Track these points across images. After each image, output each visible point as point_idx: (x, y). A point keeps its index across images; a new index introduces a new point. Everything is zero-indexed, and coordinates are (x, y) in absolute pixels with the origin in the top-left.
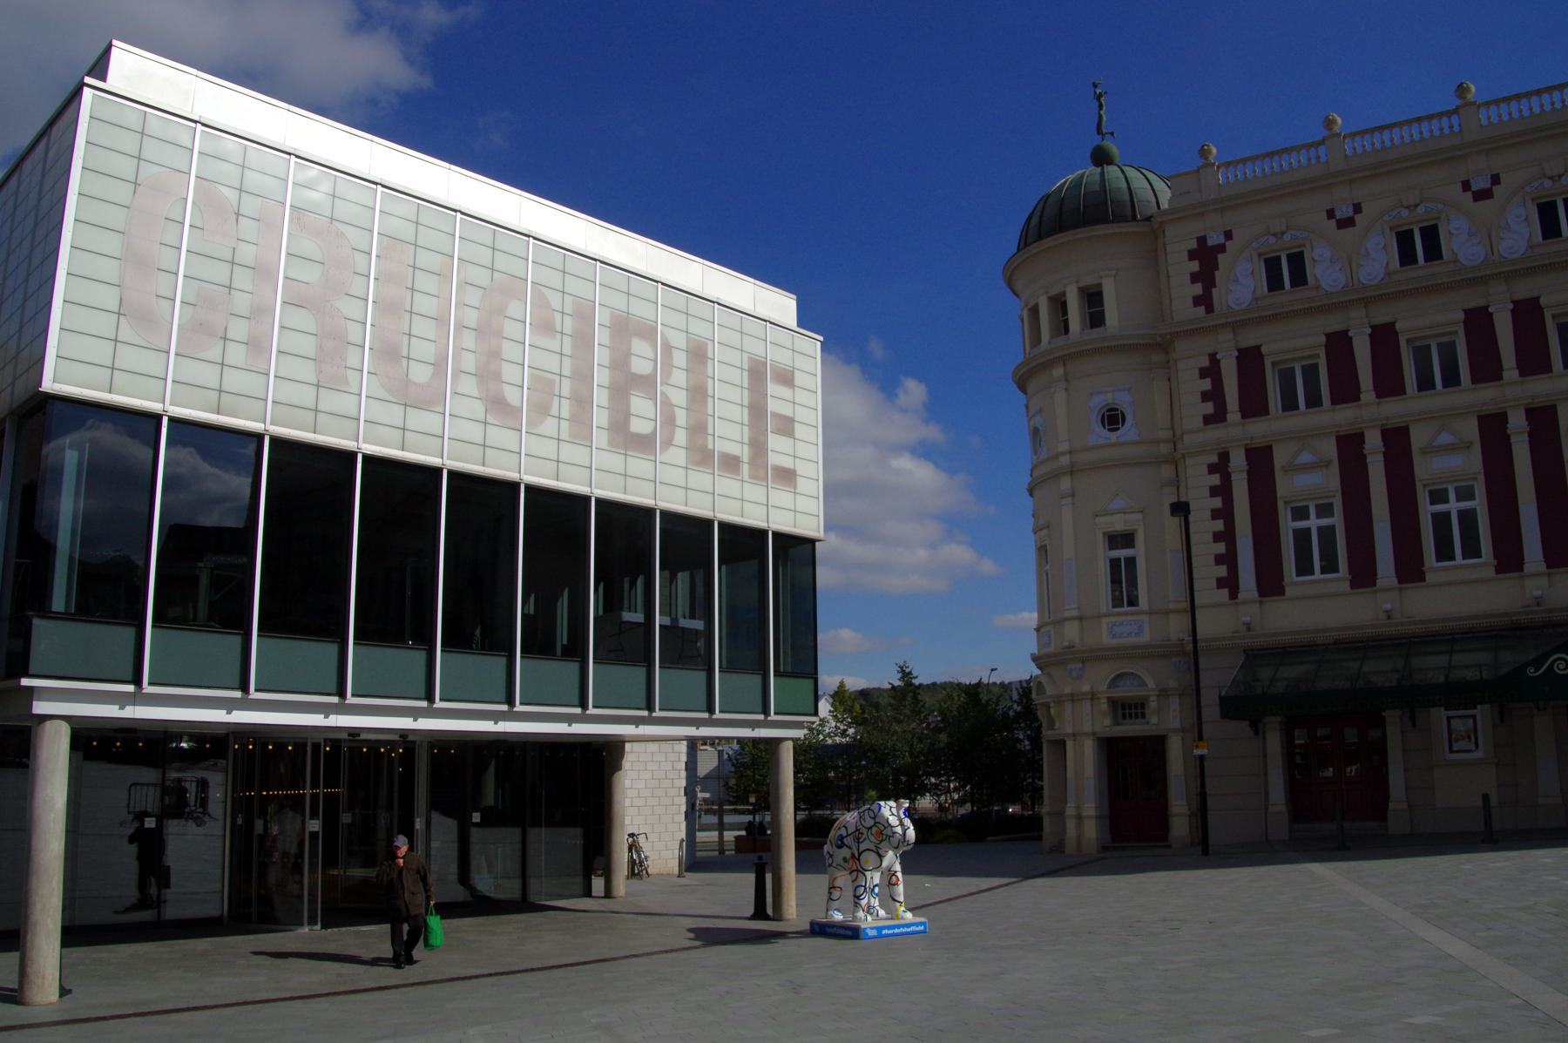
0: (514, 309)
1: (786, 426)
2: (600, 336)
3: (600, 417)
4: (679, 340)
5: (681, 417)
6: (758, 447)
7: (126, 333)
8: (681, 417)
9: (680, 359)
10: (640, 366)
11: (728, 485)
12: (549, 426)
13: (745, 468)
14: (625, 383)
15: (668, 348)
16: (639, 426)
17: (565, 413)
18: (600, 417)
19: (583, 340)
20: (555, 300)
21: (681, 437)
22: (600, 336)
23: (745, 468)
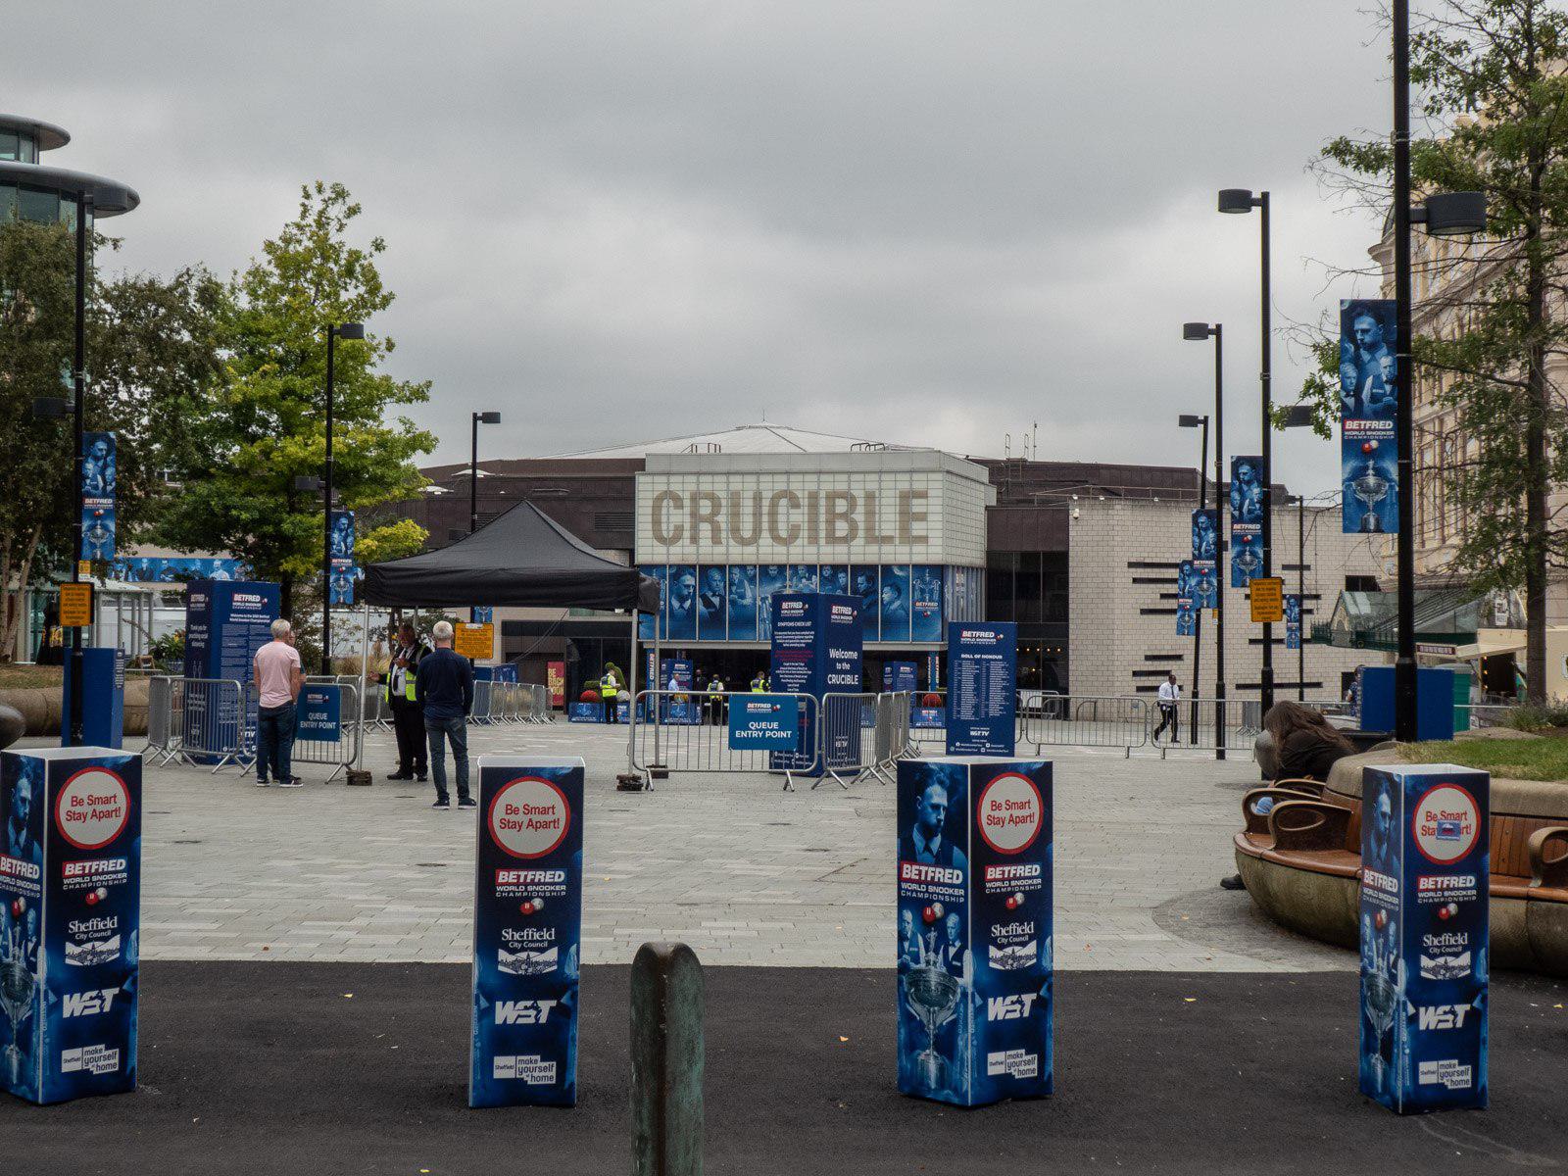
1: (922, 517)
2: (823, 502)
3: (823, 534)
4: (862, 494)
5: (861, 526)
6: (905, 529)
7: (656, 543)
8: (861, 526)
9: (861, 502)
10: (839, 510)
11: (887, 549)
12: (799, 542)
13: (897, 541)
15: (853, 498)
16: (838, 534)
17: (806, 534)
18: (823, 534)
19: (814, 506)
20: (799, 494)
21: (861, 533)
22: (823, 502)
23: (897, 541)
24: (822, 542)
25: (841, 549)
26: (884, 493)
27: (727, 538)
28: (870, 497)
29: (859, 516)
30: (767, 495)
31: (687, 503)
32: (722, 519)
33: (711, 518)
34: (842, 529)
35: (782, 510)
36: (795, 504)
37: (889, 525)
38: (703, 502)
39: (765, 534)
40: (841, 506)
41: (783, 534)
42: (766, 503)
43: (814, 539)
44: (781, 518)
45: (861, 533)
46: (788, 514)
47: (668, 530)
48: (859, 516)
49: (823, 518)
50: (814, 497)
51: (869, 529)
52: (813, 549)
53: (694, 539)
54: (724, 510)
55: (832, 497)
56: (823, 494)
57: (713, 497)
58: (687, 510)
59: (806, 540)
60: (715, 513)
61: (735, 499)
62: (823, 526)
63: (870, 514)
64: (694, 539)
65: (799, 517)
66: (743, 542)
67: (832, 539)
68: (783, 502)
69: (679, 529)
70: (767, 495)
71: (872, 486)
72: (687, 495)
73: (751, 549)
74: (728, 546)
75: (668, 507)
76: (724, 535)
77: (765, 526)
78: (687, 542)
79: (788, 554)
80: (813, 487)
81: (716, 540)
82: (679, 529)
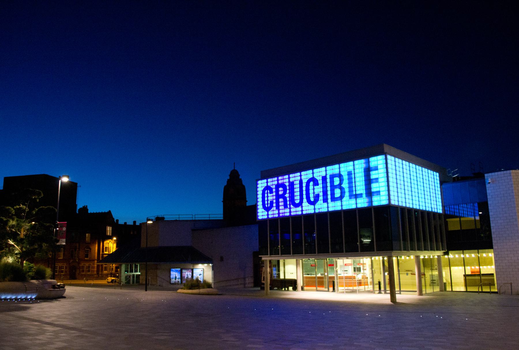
0: (311, 183)
2: (328, 180)
8: (347, 190)
14: (333, 187)
21: (347, 194)
22: (328, 180)
24: (329, 201)
25: (338, 203)
26: (356, 171)
27: (290, 205)
28: (349, 174)
29: (345, 185)
30: (305, 181)
31: (274, 190)
32: (287, 195)
33: (283, 196)
34: (338, 193)
35: (311, 187)
36: (316, 183)
37: (360, 187)
38: (281, 189)
39: (305, 200)
40: (337, 181)
41: (312, 199)
42: (304, 185)
43: (325, 200)
44: (311, 191)
45: (347, 194)
46: (314, 189)
47: (268, 204)
48: (345, 185)
49: (329, 189)
50: (324, 178)
51: (351, 191)
52: (325, 205)
53: (278, 207)
54: (288, 191)
55: (332, 177)
56: (328, 177)
57: (283, 185)
58: (274, 194)
59: (322, 201)
60: (285, 193)
61: (292, 184)
62: (329, 193)
63: (350, 183)
64: (278, 207)
65: (319, 189)
66: (296, 206)
67: (334, 199)
68: (311, 183)
69: (272, 202)
70: (305, 181)
71: (351, 168)
72: (274, 187)
73: (299, 209)
74: (290, 208)
75: (267, 193)
76: (288, 203)
77: (304, 196)
78: (274, 208)
79: (315, 209)
80: (324, 174)
81: (285, 206)
82: (272, 202)
